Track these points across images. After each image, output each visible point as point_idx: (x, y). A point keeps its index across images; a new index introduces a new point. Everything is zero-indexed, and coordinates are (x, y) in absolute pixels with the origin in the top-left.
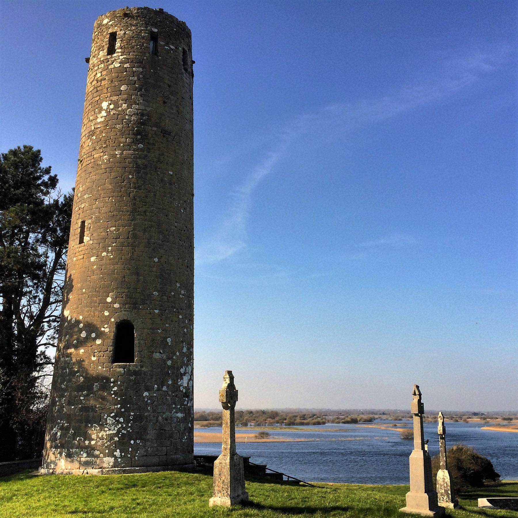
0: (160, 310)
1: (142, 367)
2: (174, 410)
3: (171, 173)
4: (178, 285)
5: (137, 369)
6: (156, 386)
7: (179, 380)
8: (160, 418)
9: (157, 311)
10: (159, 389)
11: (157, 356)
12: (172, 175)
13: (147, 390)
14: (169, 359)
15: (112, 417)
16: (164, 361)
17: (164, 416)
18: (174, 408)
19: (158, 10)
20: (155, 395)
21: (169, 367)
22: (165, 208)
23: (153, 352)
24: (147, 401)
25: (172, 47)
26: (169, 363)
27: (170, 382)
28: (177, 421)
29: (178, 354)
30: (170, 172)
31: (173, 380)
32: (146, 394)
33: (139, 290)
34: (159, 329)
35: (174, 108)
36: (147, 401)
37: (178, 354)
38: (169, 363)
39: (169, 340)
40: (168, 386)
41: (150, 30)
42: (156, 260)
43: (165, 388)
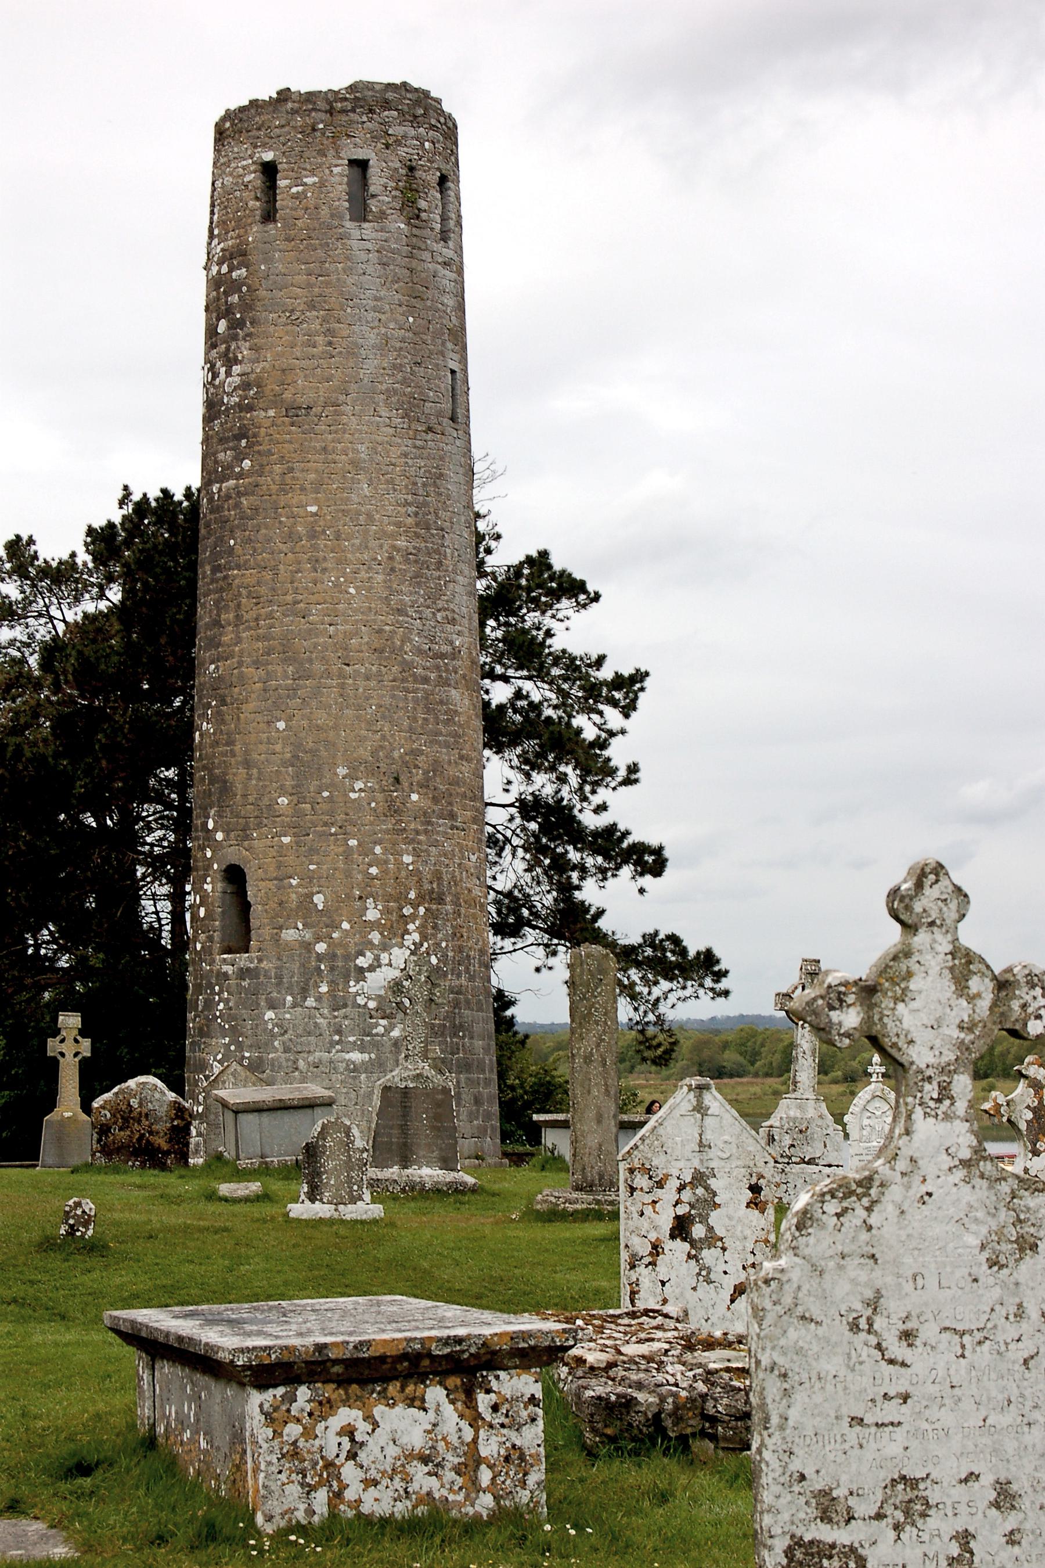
0: (295, 835)
1: (260, 960)
2: (338, 1047)
3: (313, 509)
4: (342, 771)
5: (252, 965)
6: (289, 998)
7: (352, 983)
8: (301, 1063)
9: (286, 840)
10: (294, 1006)
11: (289, 935)
12: (316, 514)
13: (272, 1006)
14: (319, 939)
15: (219, 1062)
16: (308, 947)
17: (311, 1059)
18: (338, 1043)
19: (275, 96)
20: (288, 1016)
21: (320, 958)
22: (300, 597)
23: (281, 928)
24: (272, 1030)
25: (309, 180)
26: (321, 947)
27: (324, 989)
28: (347, 1069)
29: (346, 926)
30: (309, 509)
31: (332, 983)
32: (270, 1015)
33: (251, 799)
34: (290, 877)
35: (320, 340)
36: (272, 1030)
37: (346, 926)
38: (321, 947)
39: (319, 900)
40: (319, 999)
41: (260, 161)
42: (281, 725)
43: (310, 1002)
